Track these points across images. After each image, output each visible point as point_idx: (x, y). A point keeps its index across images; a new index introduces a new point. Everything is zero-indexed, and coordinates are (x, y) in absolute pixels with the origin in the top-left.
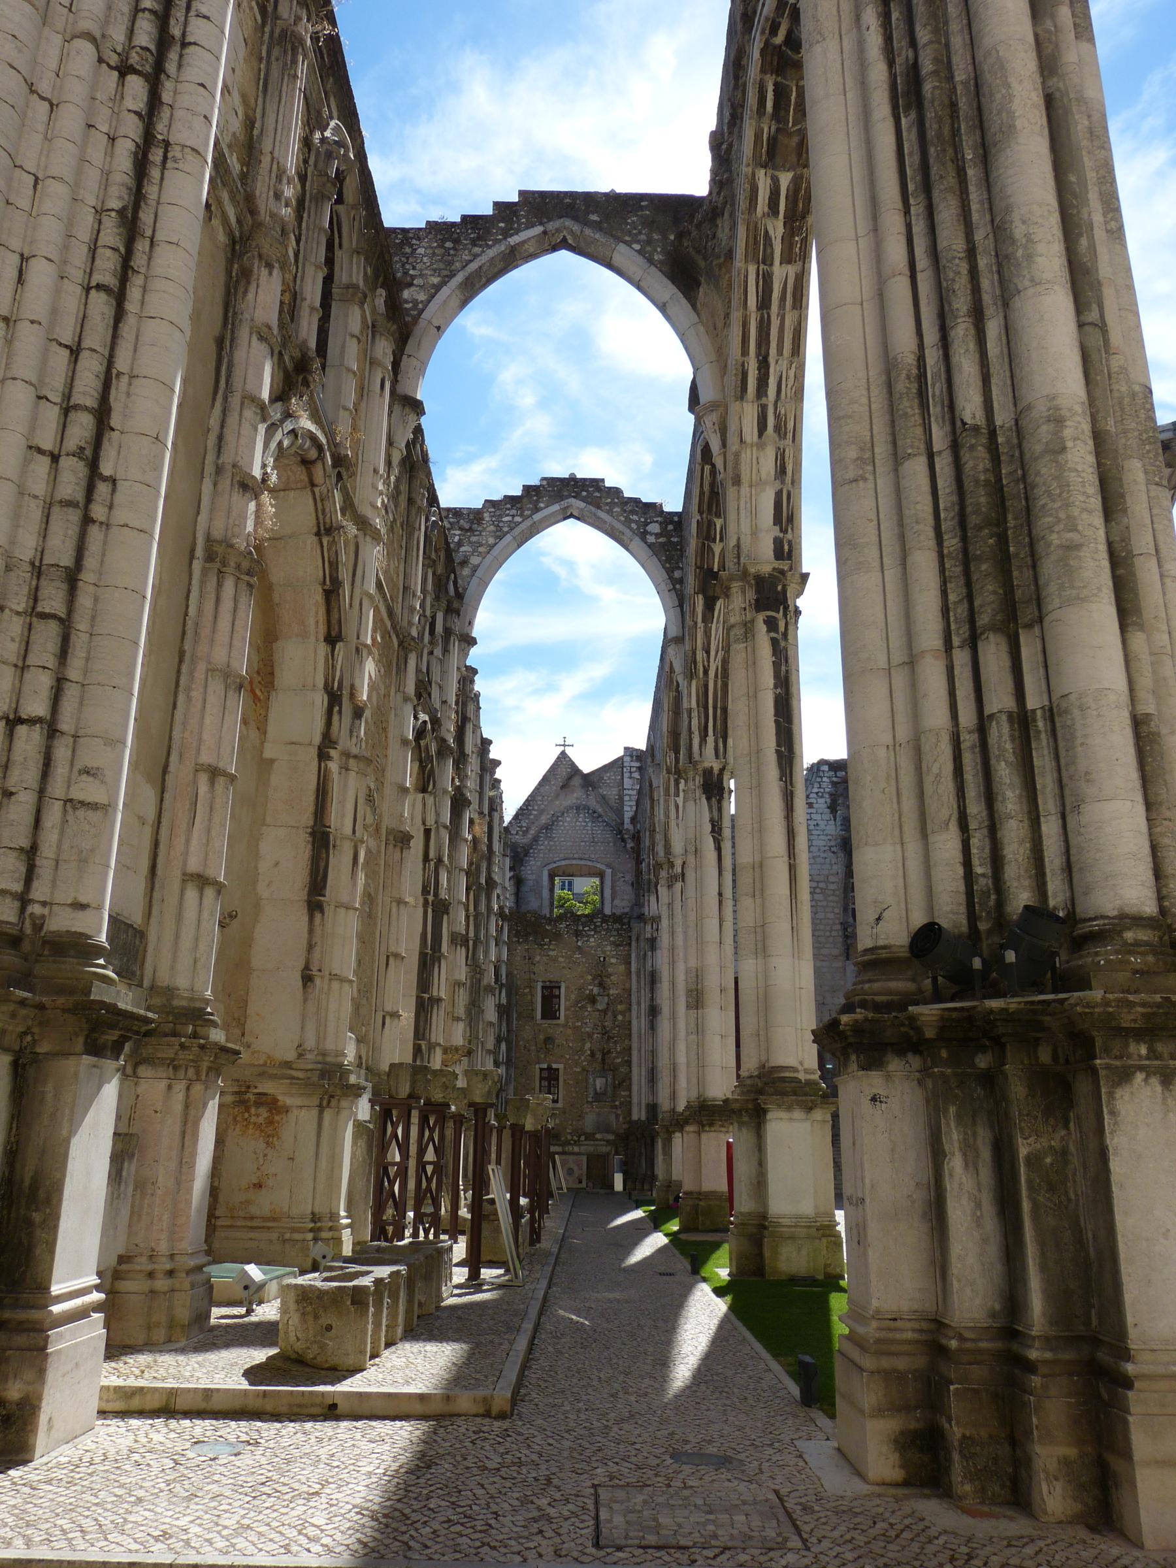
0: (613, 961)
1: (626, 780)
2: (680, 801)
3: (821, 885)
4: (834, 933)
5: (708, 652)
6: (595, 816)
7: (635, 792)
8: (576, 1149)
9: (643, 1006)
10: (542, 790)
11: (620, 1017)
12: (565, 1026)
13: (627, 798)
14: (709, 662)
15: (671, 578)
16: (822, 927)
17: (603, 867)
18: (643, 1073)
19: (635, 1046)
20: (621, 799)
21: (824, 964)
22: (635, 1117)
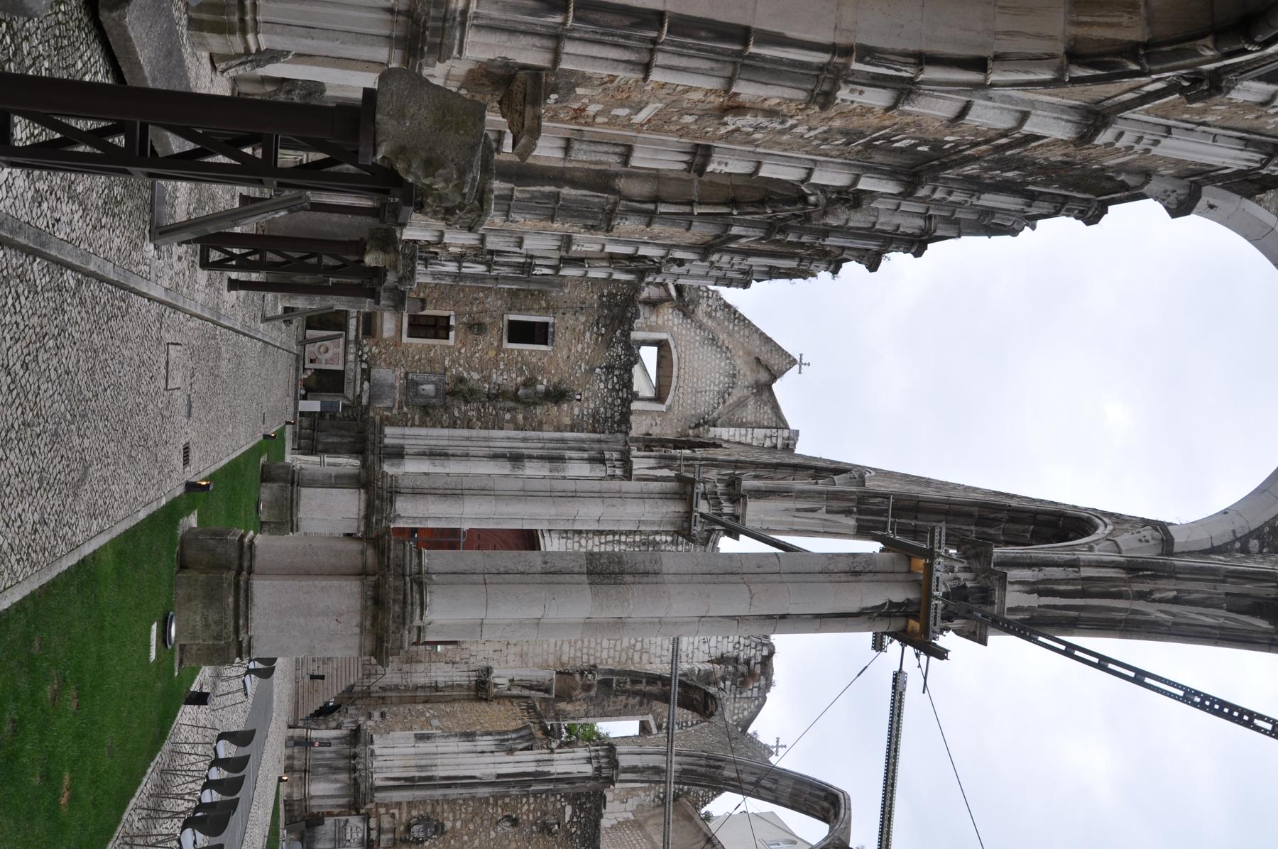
0: (576, 411)
1: (763, 431)
2: (822, 514)
3: (639, 646)
4: (585, 657)
5: (1175, 601)
6: (723, 395)
7: (749, 441)
8: (351, 357)
9: (521, 445)
10: (756, 336)
11: (508, 416)
12: (499, 349)
13: (743, 431)
14: (1161, 601)
15: (1251, 534)
16: (593, 645)
17: (668, 402)
18: (441, 443)
19: (474, 433)
21: (552, 645)
22: (388, 430)
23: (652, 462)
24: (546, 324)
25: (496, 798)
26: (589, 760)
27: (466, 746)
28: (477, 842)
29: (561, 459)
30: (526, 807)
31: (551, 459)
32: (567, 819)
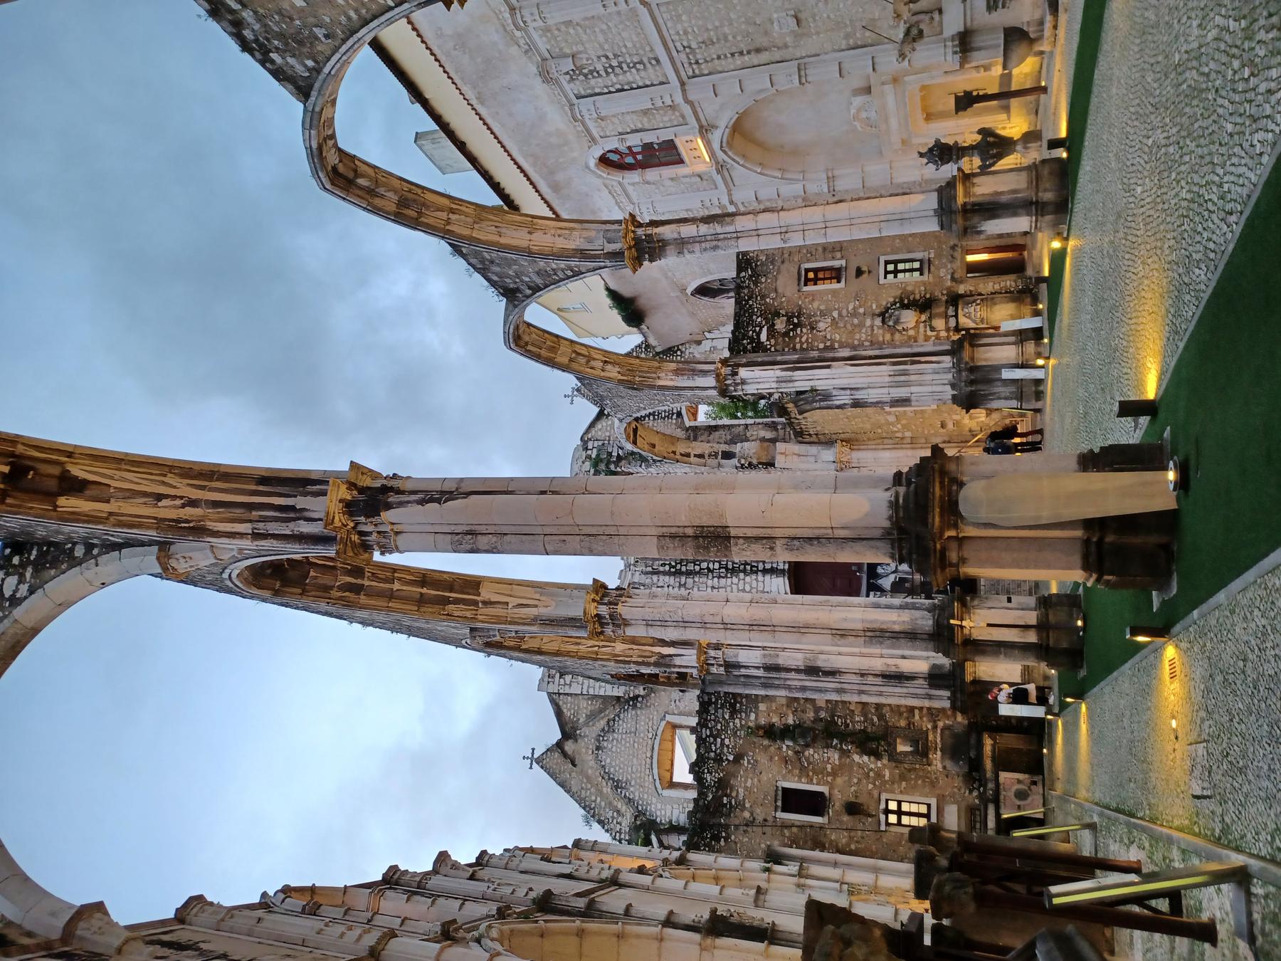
0: (753, 716)
5: (160, 497)
6: (610, 728)
7: (586, 682)
9: (807, 684)
13: (591, 692)
14: (174, 497)
15: (79, 562)
17: (663, 723)
18: (890, 689)
19: (855, 698)
20: (595, 697)
23: (677, 661)
24: (784, 810)
25: (832, 348)
26: (743, 382)
27: (859, 395)
28: (851, 307)
29: (768, 668)
30: (804, 339)
31: (776, 668)
32: (765, 329)
